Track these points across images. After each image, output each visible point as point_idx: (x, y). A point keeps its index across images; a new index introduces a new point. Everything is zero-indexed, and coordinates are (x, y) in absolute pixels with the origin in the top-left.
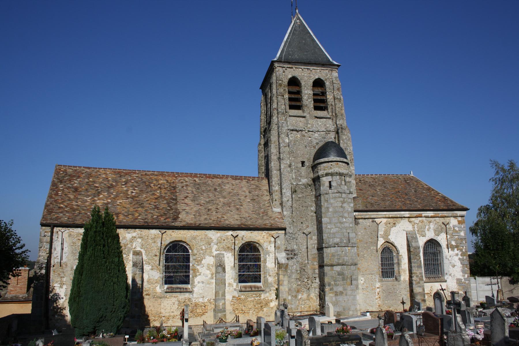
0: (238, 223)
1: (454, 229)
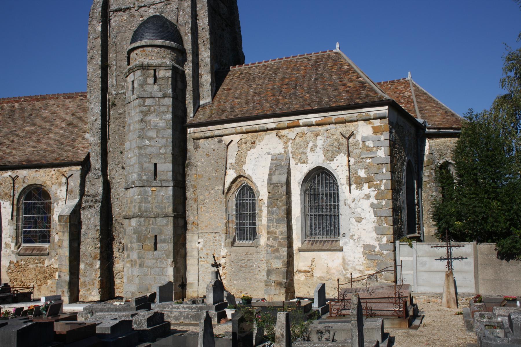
0: (27, 161)
1: (364, 145)
